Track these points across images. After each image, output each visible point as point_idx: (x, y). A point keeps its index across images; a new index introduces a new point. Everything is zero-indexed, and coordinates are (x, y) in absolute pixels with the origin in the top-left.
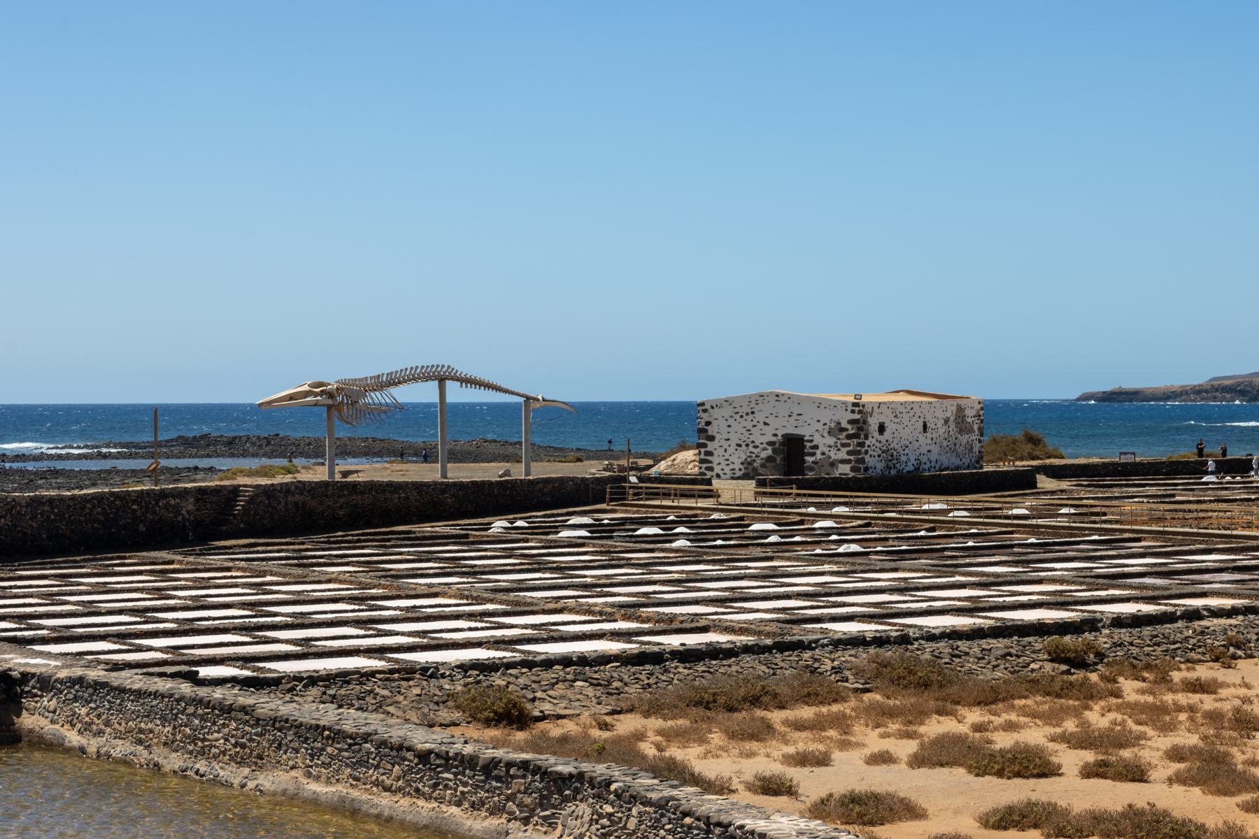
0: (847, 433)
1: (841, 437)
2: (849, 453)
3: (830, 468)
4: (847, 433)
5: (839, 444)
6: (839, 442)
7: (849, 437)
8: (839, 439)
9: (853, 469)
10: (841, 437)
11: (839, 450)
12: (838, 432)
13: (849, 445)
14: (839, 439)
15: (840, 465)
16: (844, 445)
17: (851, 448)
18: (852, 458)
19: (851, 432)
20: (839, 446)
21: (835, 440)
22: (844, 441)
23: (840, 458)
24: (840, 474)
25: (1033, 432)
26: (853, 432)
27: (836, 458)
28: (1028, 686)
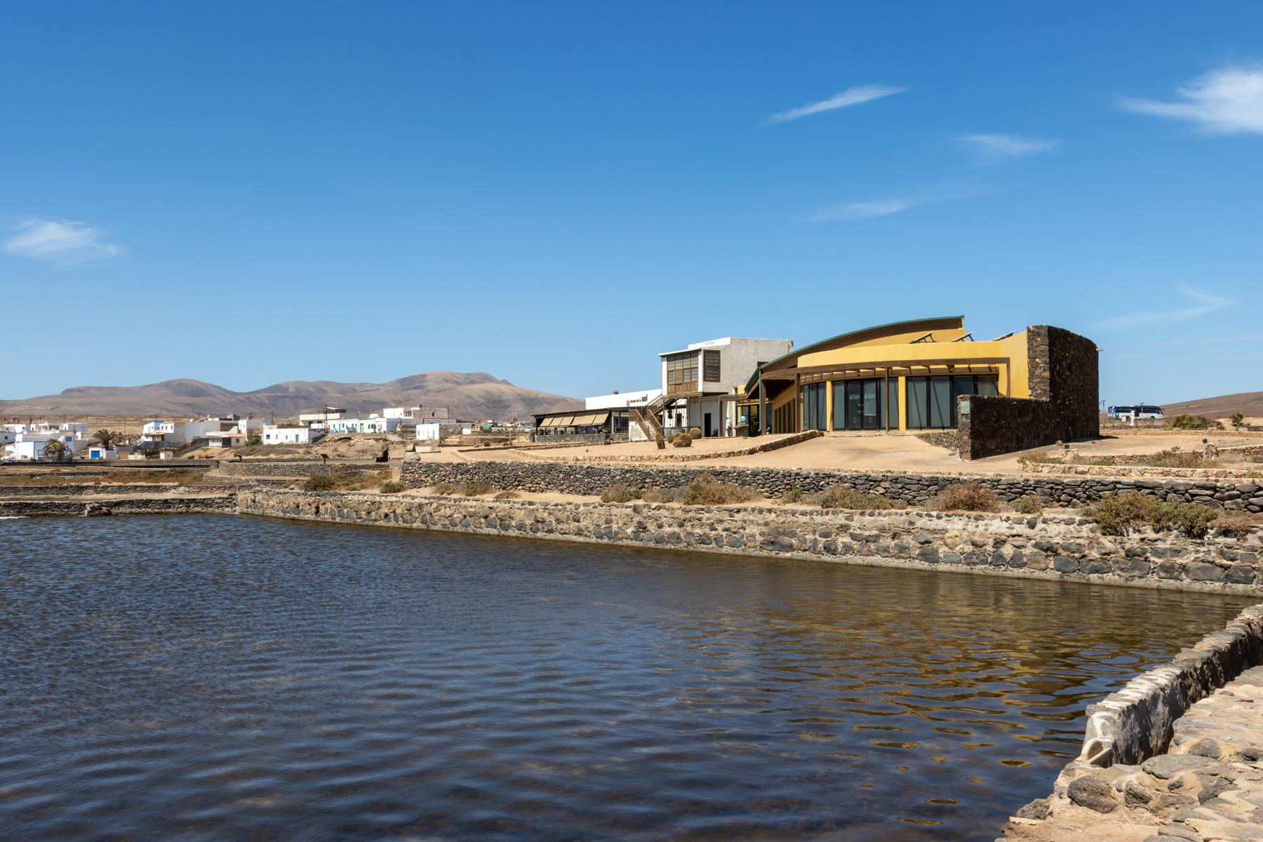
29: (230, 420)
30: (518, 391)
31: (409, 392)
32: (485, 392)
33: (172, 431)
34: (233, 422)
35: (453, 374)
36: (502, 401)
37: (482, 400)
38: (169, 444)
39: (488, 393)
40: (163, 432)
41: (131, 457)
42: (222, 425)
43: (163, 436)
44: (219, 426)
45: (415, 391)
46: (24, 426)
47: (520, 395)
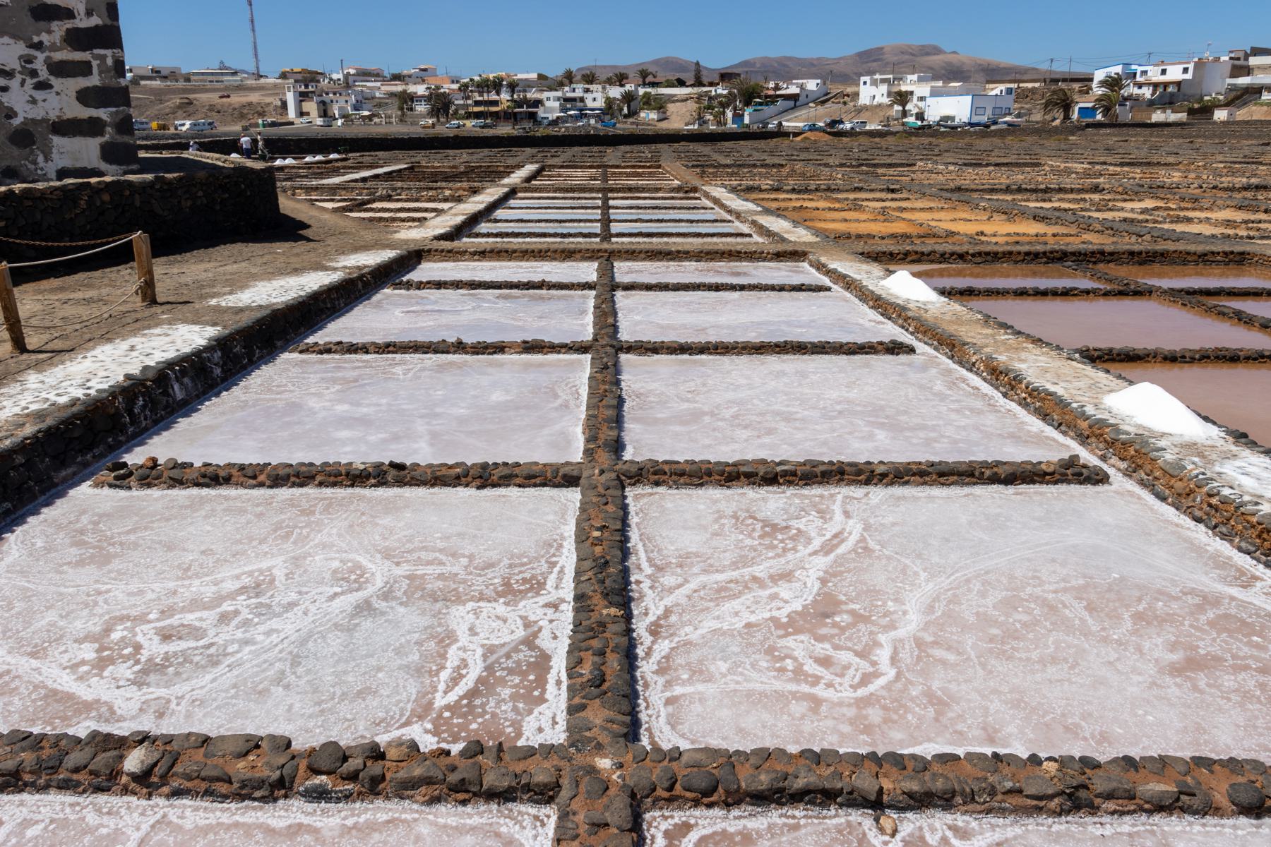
0: (69, 24)
1: (45, 38)
2: (85, 97)
3: (16, 151)
4: (69, 24)
5: (39, 64)
6: (41, 57)
7: (77, 39)
8: (39, 46)
9: (109, 153)
10: (45, 38)
11: (43, 86)
12: (28, 19)
13: (83, 69)
14: (39, 46)
15: (57, 140)
16: (61, 69)
17: (94, 80)
18: (103, 114)
19: (83, 22)
20: (44, 74)
21: (20, 49)
22: (59, 56)
23: (53, 116)
24: (62, 174)
25: (423, 67)
26: (95, 21)
27: (37, 113)
28: (776, 673)
29: (1238, 59)
30: (978, 62)
31: (870, 64)
32: (946, 63)
33: (1189, 76)
34: (1241, 62)
35: (909, 46)
36: (962, 72)
37: (943, 72)
38: (1187, 98)
39: (949, 64)
40: (1157, 78)
41: (1158, 116)
42: (1234, 67)
43: (1179, 84)
44: (1228, 69)
45: (875, 64)
46: (819, 81)
47: (980, 65)
